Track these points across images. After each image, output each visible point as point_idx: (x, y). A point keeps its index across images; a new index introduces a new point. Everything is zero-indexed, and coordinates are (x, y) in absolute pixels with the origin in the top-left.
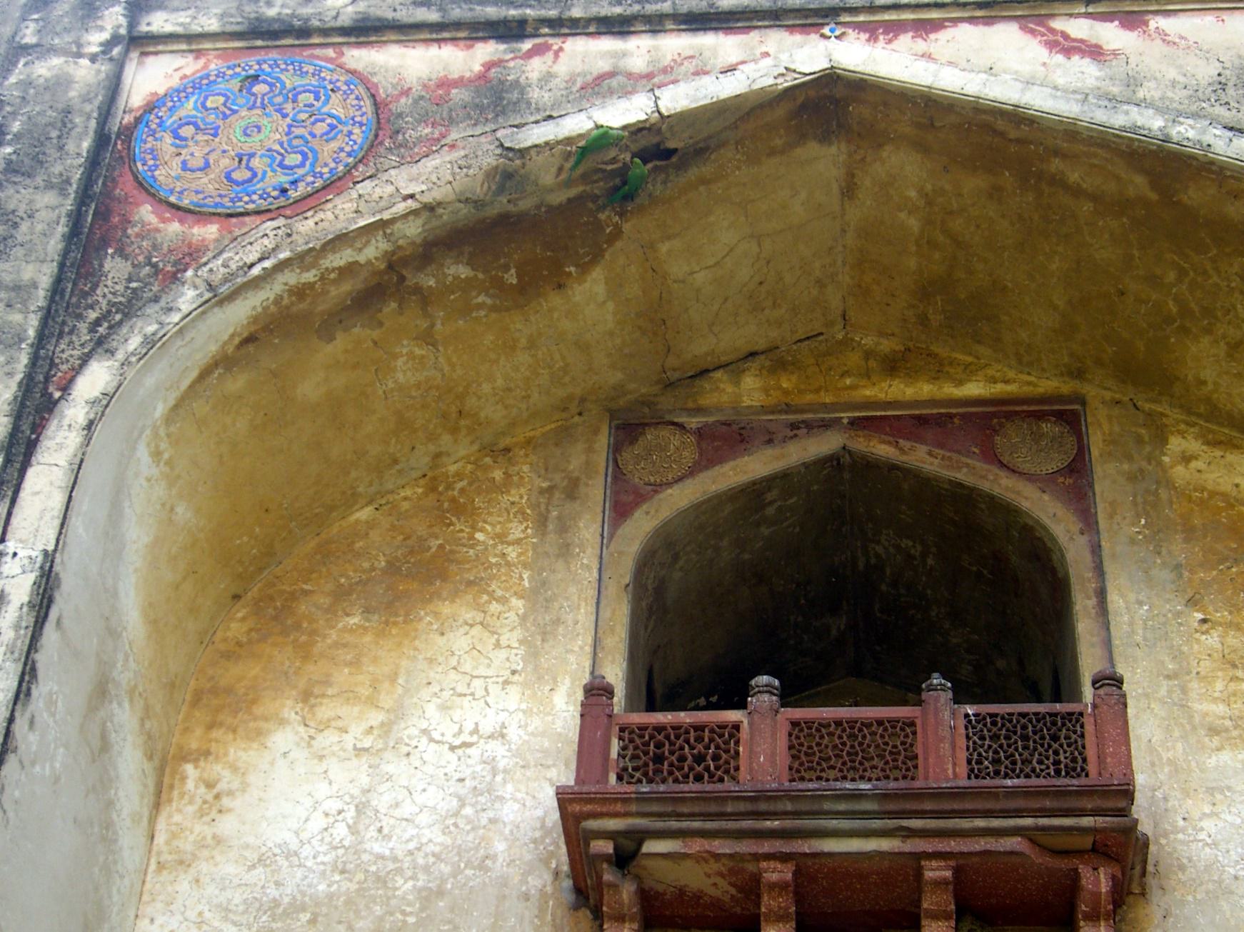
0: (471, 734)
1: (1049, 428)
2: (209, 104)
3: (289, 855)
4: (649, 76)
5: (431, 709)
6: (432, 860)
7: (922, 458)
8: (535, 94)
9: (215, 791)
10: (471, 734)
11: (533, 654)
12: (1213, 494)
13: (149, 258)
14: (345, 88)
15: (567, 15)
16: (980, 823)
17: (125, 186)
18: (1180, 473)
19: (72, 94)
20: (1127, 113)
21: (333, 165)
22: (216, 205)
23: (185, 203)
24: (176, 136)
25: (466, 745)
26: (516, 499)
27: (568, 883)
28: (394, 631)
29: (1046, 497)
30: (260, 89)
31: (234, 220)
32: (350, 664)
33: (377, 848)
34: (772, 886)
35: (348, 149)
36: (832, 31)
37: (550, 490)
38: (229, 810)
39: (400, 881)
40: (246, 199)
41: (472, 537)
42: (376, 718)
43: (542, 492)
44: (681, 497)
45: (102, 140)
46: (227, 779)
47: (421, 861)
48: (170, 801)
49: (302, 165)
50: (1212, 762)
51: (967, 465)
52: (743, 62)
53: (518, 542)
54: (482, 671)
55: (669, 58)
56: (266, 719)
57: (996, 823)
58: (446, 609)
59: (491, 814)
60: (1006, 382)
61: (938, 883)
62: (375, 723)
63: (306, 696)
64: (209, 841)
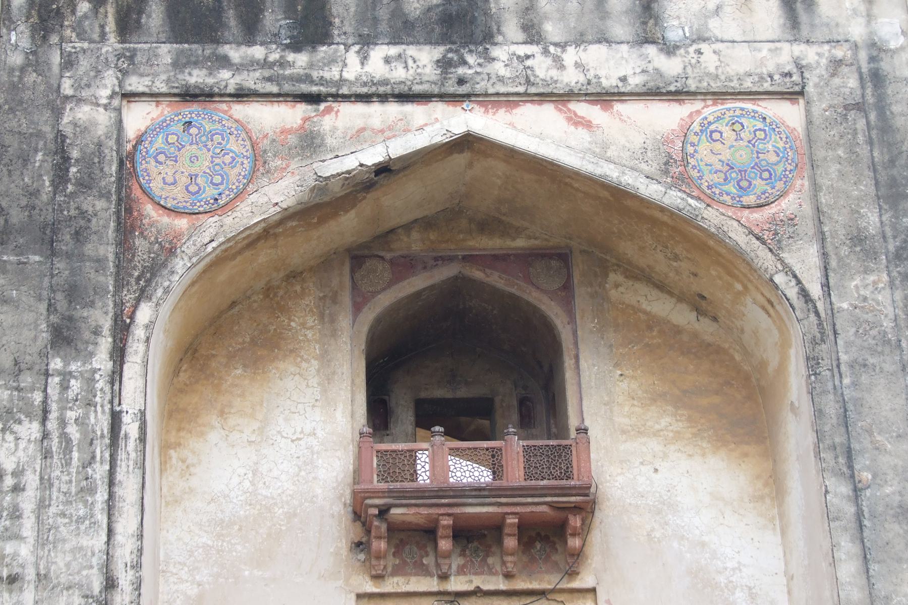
0: (301, 433)
1: (554, 263)
2: (170, 141)
3: (226, 496)
4: (382, 131)
5: (281, 420)
6: (289, 498)
7: (496, 279)
8: (329, 141)
9: (186, 464)
10: (301, 433)
11: (324, 391)
12: (628, 306)
13: (157, 238)
14: (235, 132)
15: (340, 92)
16: (530, 500)
17: (137, 192)
18: (613, 294)
19: (100, 133)
20: (602, 167)
21: (237, 184)
22: (184, 207)
23: (169, 205)
24: (157, 161)
25: (300, 439)
26: (308, 303)
27: (350, 509)
28: (259, 378)
29: (553, 303)
30: (193, 131)
31: (194, 216)
32: (240, 396)
33: (264, 492)
34: (444, 526)
35: (243, 174)
36: (468, 106)
37: (325, 296)
38: (195, 474)
39: (277, 509)
40: (198, 204)
41: (289, 325)
42: (256, 425)
43: (320, 299)
44: (385, 300)
45: (121, 163)
46: (191, 459)
47: (284, 498)
48: (166, 470)
49: (222, 183)
50: (622, 448)
51: (517, 284)
52: (426, 125)
53: (311, 328)
54: (302, 400)
55: (391, 119)
56: (205, 426)
57: (536, 500)
58: (282, 365)
59: (313, 475)
60: (536, 239)
61: (512, 525)
62: (255, 428)
63: (222, 413)
64: (187, 490)
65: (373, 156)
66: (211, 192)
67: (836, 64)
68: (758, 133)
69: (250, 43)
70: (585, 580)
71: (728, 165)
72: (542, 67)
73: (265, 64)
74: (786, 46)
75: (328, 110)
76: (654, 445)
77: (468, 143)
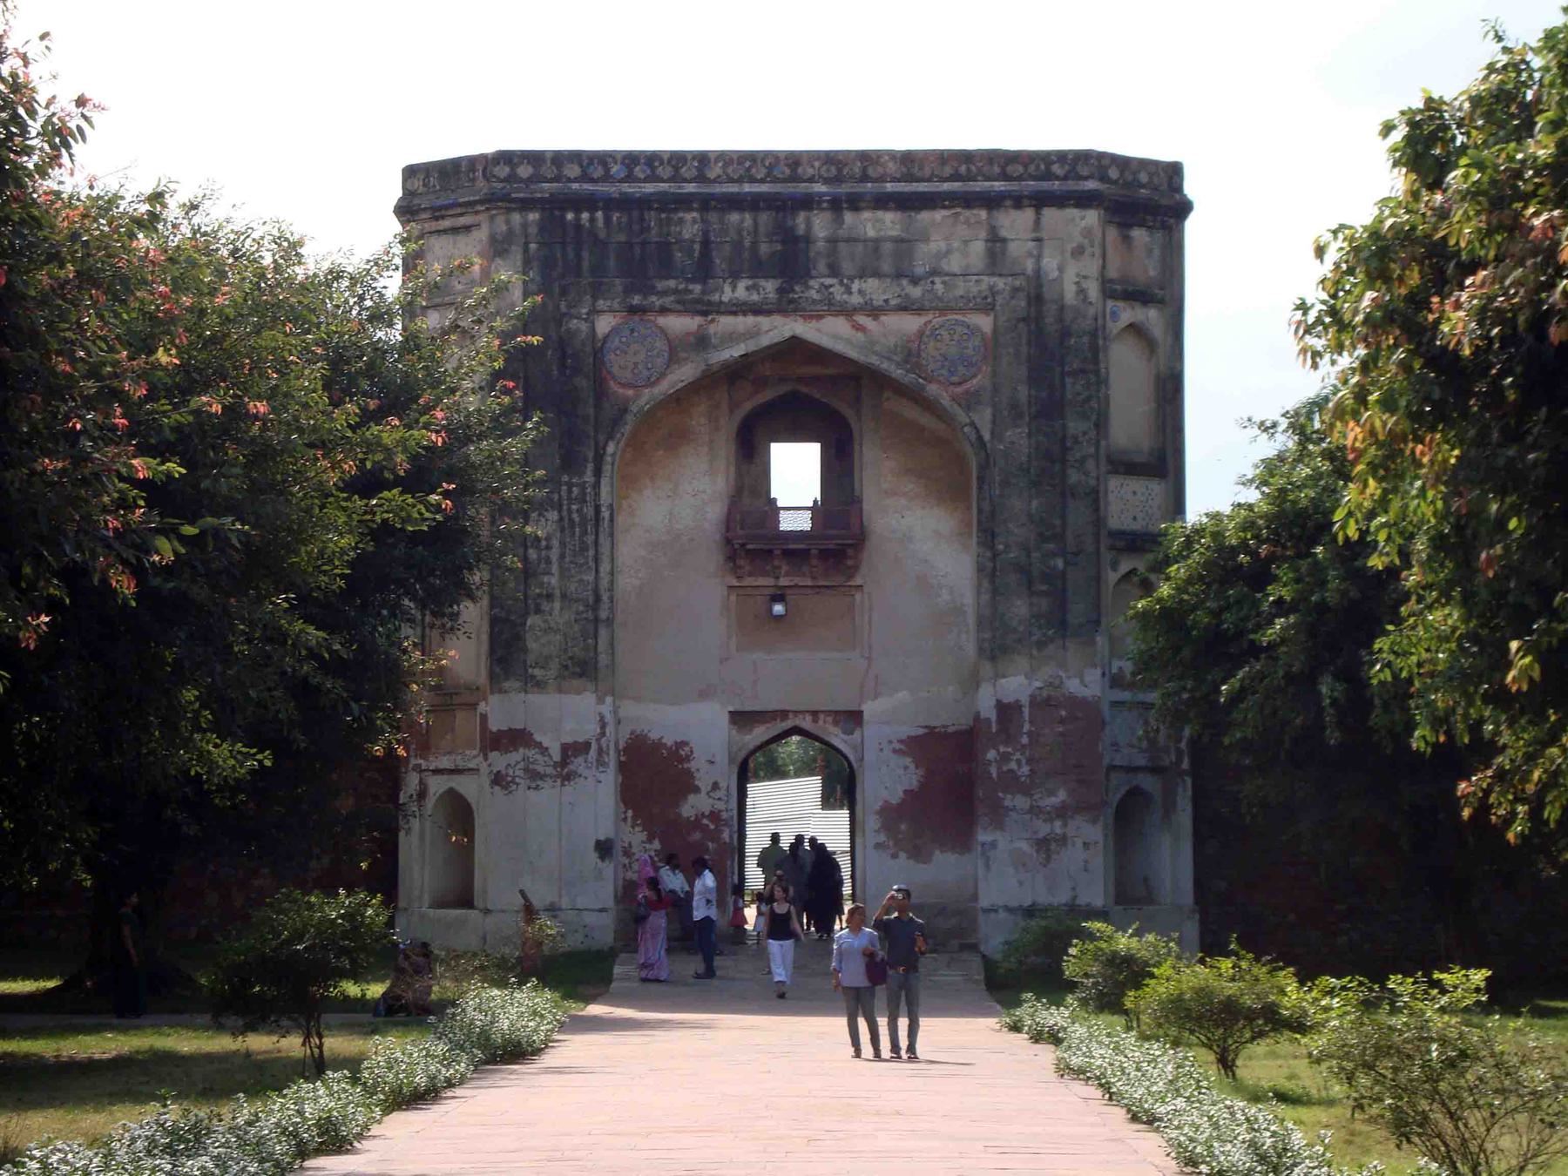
44: (748, 406)
63: (652, 479)
65: (737, 351)
66: (646, 373)
67: (1016, 290)
69: (667, 279)
70: (858, 581)
72: (838, 292)
73: (676, 291)
74: (986, 278)
75: (713, 321)
76: (903, 501)
77: (795, 343)
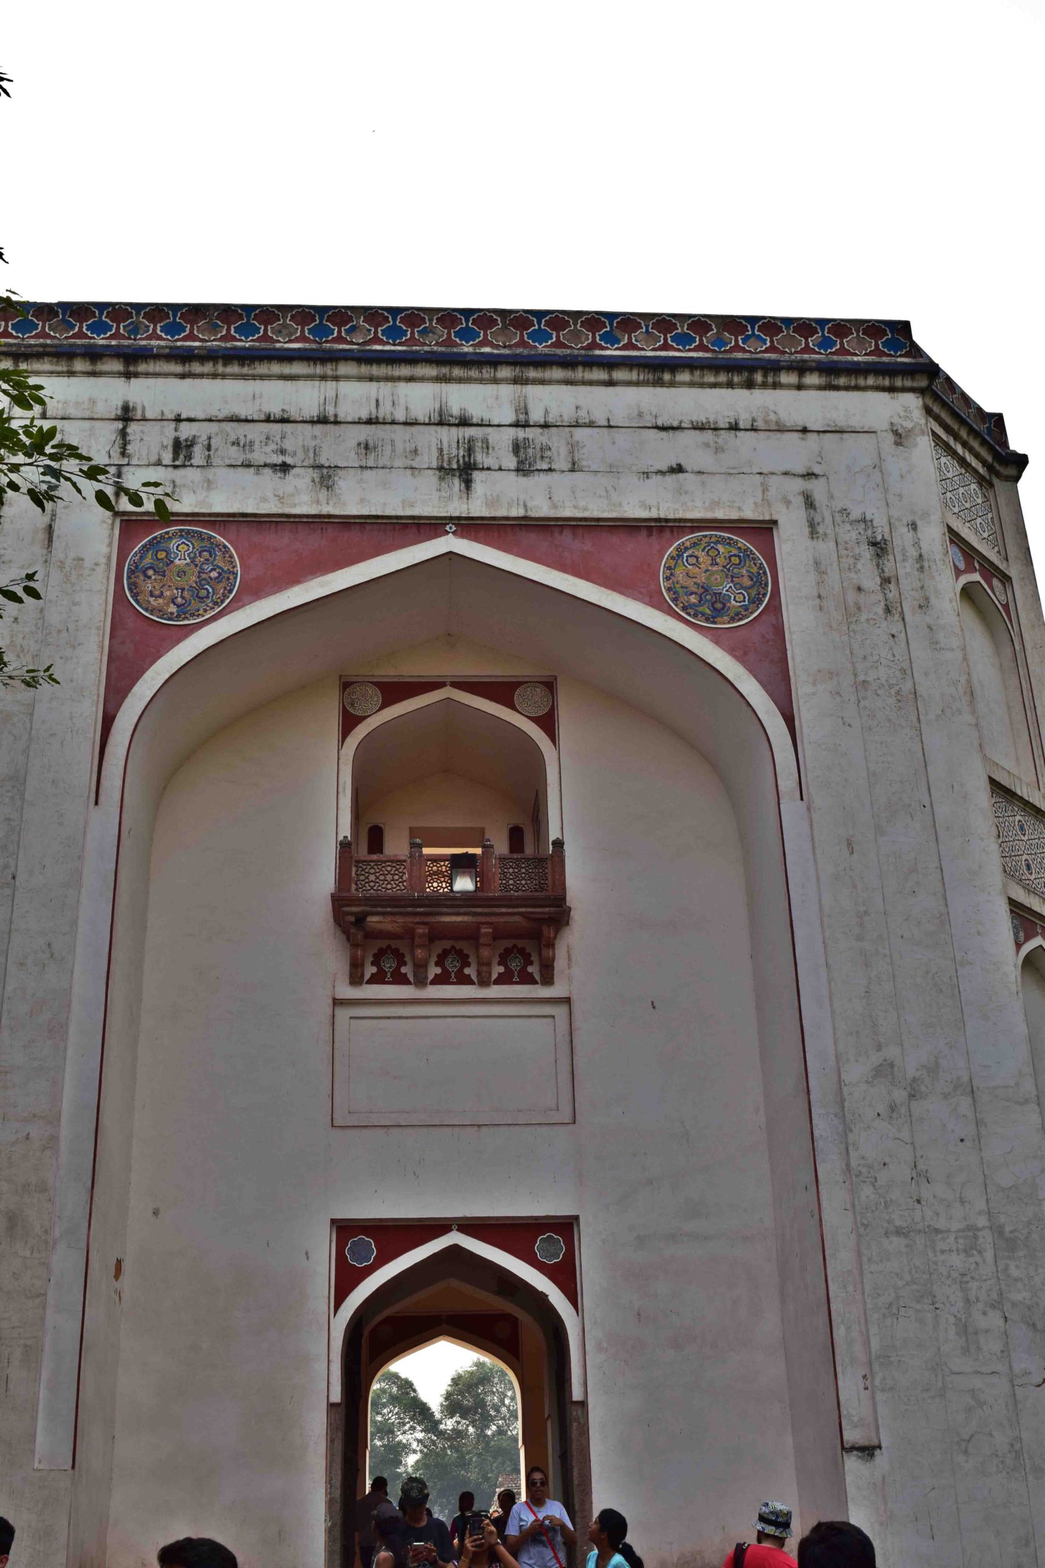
16: (504, 910)
57: (510, 910)
61: (486, 934)
68: (733, 558)
71: (703, 587)
